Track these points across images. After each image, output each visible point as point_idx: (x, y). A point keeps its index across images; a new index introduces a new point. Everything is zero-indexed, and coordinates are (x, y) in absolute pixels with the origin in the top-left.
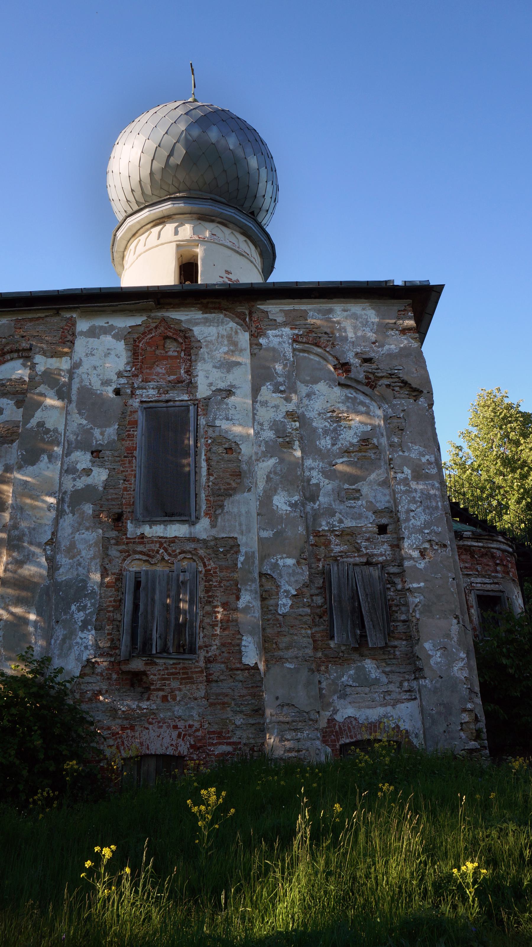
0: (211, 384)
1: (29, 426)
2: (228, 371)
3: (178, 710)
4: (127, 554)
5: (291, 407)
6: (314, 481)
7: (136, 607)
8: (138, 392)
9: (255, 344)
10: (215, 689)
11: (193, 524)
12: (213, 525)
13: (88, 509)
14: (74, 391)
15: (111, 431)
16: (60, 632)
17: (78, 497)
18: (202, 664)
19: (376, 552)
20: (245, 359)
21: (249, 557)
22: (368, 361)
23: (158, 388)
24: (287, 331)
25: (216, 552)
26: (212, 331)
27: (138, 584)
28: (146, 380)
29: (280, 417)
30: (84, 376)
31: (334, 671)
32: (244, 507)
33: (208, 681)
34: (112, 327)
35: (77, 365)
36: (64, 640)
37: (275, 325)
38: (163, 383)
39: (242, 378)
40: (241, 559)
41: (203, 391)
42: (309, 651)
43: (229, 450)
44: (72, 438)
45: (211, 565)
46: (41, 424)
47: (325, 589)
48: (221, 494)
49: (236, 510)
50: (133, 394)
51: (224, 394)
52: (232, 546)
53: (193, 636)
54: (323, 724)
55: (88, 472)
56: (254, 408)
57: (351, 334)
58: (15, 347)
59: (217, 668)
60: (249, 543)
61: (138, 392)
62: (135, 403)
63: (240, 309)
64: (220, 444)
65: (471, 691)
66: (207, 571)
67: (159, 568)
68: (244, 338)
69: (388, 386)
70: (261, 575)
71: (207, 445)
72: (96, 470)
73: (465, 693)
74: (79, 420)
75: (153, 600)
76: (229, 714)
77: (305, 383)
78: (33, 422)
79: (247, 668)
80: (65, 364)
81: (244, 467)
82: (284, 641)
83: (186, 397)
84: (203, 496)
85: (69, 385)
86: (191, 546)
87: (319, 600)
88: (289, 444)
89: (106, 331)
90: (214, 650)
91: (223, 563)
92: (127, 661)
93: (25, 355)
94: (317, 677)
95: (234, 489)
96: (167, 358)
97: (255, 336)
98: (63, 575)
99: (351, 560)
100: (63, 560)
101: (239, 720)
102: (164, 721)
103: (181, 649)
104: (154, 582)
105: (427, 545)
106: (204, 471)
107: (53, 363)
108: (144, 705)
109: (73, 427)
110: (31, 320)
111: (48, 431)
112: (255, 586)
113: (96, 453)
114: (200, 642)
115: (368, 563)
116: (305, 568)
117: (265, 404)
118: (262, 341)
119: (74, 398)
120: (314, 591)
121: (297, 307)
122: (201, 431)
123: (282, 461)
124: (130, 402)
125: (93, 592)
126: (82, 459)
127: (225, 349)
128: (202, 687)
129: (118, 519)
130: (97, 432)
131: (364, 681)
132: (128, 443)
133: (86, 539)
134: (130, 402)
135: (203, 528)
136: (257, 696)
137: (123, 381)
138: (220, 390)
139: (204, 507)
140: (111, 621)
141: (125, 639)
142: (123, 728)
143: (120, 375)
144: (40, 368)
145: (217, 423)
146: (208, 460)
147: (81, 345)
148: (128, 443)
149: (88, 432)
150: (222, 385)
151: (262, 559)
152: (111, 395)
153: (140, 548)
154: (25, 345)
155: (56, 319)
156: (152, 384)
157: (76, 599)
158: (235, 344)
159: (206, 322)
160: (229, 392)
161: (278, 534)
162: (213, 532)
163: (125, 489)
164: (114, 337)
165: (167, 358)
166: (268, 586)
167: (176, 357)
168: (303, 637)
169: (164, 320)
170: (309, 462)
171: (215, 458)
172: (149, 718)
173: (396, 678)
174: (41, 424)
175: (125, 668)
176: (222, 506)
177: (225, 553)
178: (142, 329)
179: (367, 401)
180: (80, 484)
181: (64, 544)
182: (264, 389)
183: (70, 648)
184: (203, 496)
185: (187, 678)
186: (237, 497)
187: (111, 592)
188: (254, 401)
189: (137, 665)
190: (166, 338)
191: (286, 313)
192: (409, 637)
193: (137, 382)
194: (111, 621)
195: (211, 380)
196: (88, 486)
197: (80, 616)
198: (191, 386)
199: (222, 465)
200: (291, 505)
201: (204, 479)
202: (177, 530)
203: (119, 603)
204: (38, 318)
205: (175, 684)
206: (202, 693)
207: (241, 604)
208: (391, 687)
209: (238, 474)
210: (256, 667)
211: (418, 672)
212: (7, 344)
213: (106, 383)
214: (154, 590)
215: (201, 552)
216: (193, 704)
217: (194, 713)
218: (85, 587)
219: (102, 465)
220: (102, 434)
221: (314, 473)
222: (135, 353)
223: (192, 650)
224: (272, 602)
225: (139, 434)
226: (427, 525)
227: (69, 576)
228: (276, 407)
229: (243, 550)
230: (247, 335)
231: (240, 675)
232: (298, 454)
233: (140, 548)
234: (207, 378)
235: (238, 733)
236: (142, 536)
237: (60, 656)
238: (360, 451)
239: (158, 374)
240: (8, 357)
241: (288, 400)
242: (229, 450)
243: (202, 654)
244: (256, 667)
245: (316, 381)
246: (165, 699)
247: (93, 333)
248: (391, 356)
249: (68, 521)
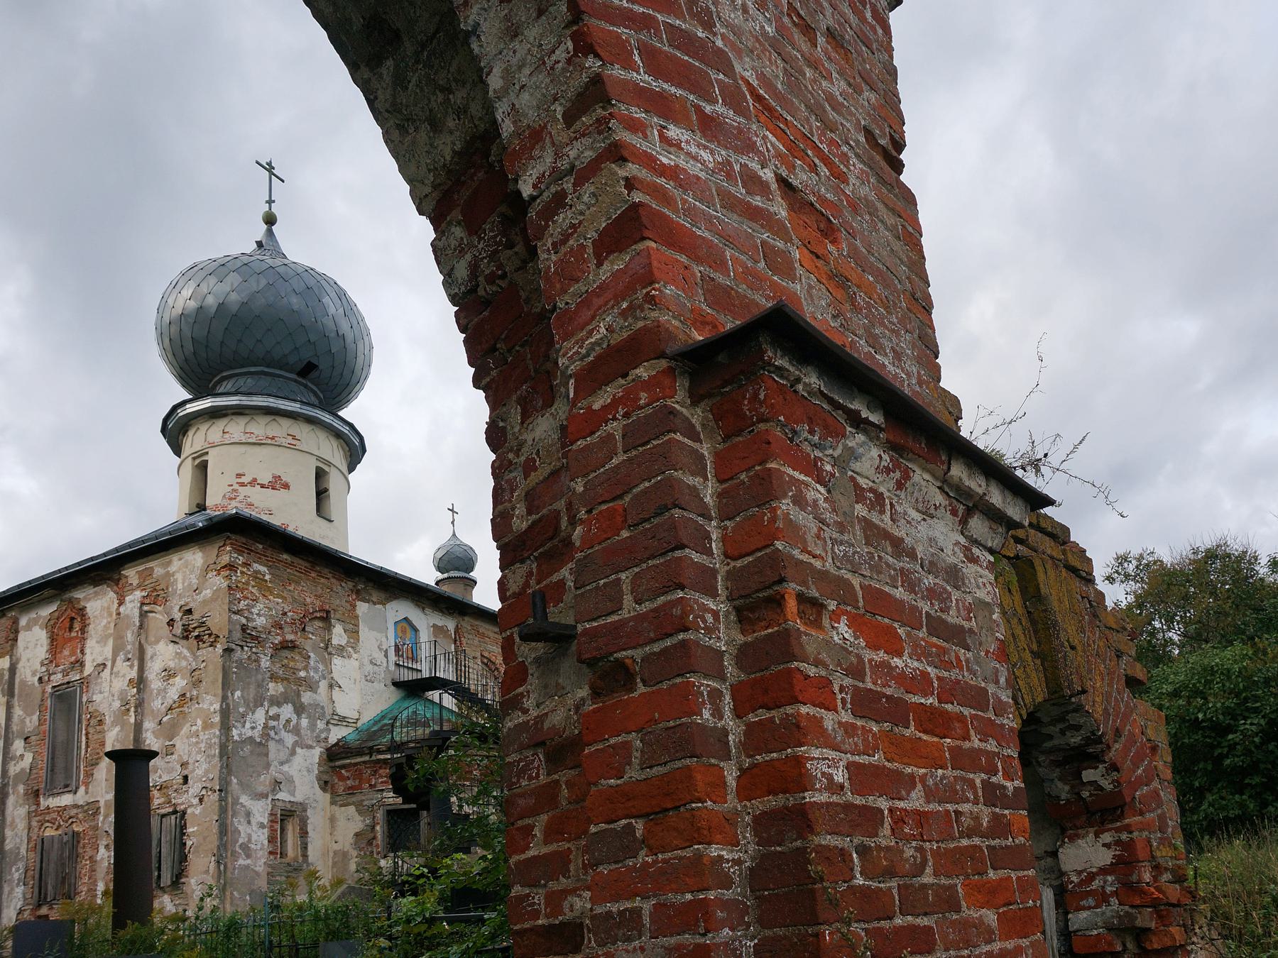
19: (180, 801)
22: (189, 612)
41: (88, 669)
57: (180, 586)
62: (49, 689)
69: (197, 637)
97: (120, 604)
105: (204, 792)
137: (44, 669)
138: (99, 665)
146: (87, 734)
150: (100, 661)
152: (37, 684)
171: (91, 730)
198: (80, 664)
226: (207, 772)
236: (48, 808)
245: (157, 642)
248: (205, 602)
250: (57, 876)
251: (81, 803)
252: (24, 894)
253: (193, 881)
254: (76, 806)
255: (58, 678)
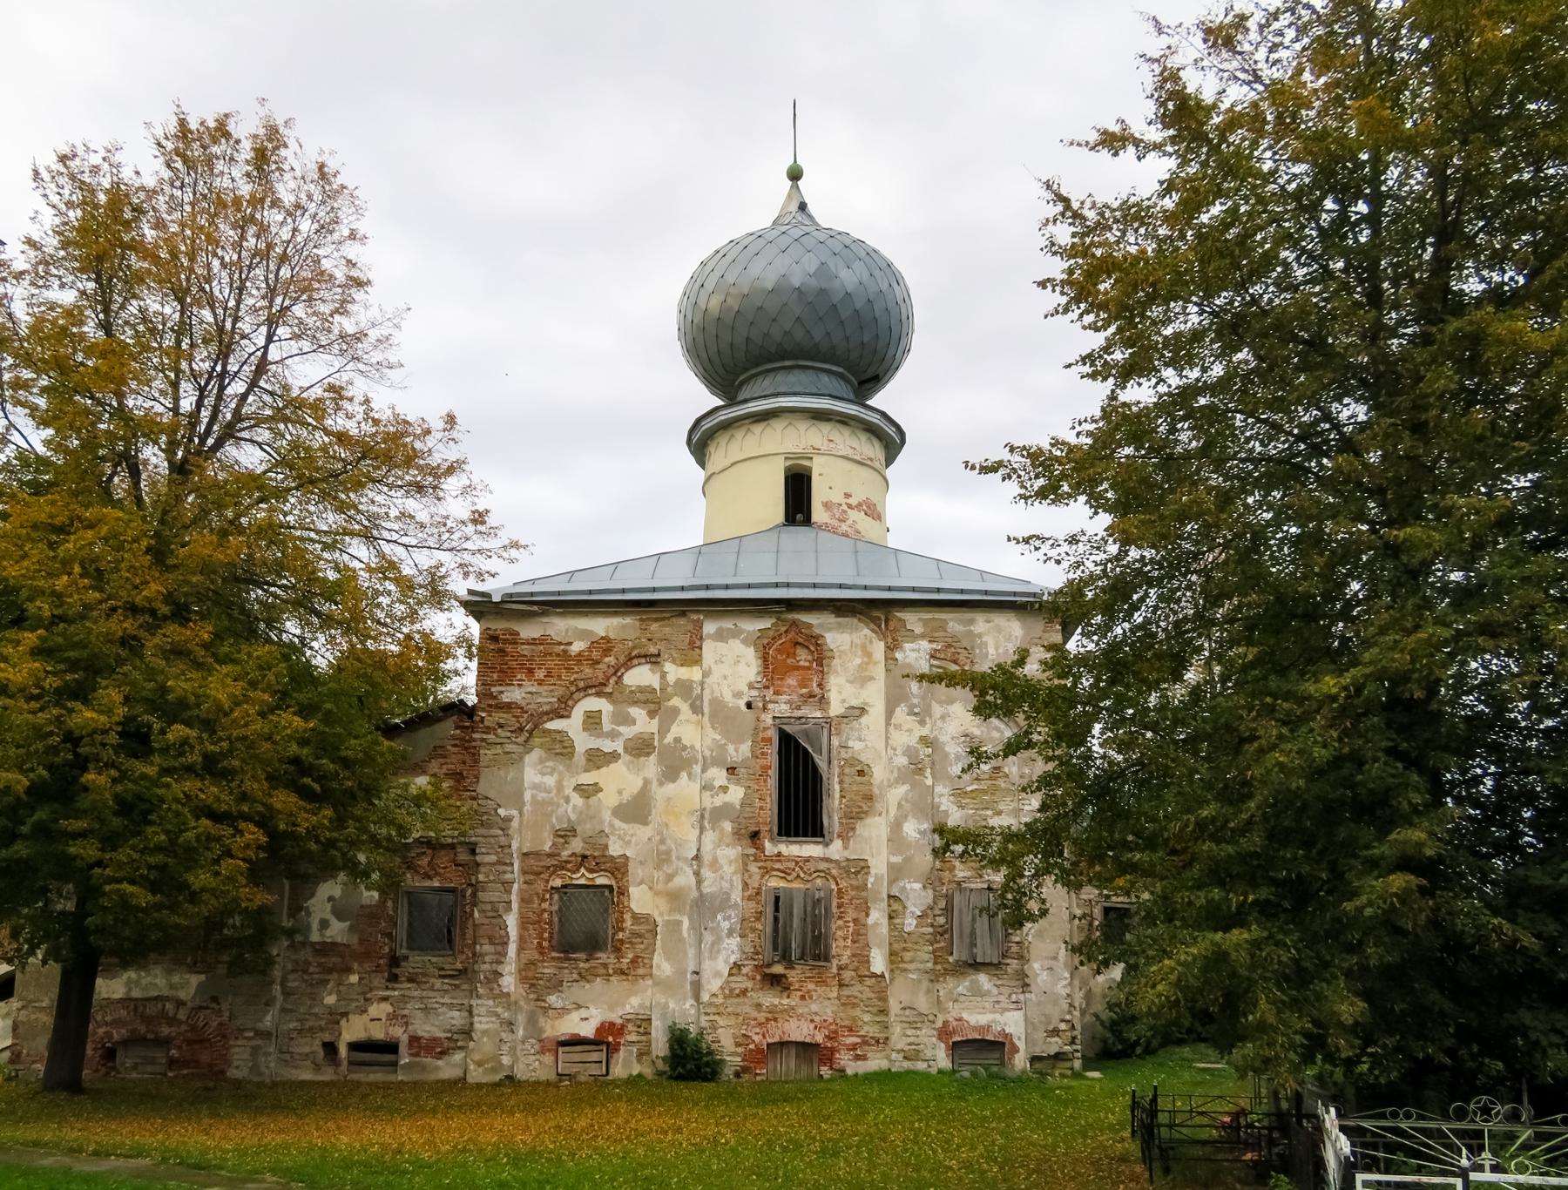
0: (844, 701)
1: (666, 741)
2: (862, 686)
3: (814, 1007)
4: (766, 871)
5: (925, 731)
6: (943, 808)
7: (776, 919)
8: (770, 706)
9: (890, 659)
10: (846, 992)
11: (827, 845)
12: (845, 848)
13: (728, 826)
14: (706, 703)
15: (745, 748)
16: (708, 938)
17: (718, 814)
18: (835, 970)
20: (879, 672)
21: (878, 878)
23: (789, 702)
24: (925, 645)
25: (848, 872)
26: (845, 641)
27: (777, 899)
28: (776, 693)
29: (913, 741)
30: (715, 687)
31: (951, 982)
32: (874, 830)
33: (841, 985)
34: (741, 631)
35: (706, 674)
36: (712, 945)
37: (914, 637)
38: (795, 697)
39: (874, 696)
40: (871, 880)
41: (836, 709)
42: (930, 965)
43: (861, 773)
44: (707, 753)
45: (843, 884)
46: (677, 740)
47: (948, 910)
48: (855, 816)
49: (866, 834)
50: (765, 708)
51: (857, 712)
52: (863, 867)
53: (828, 947)
54: (939, 1024)
55: (724, 789)
56: (887, 732)
58: (643, 652)
59: (847, 975)
60: (879, 866)
61: (770, 706)
63: (875, 614)
64: (852, 766)
65: (1071, 1005)
66: (840, 890)
67: (796, 885)
68: (879, 648)
70: (890, 897)
71: (841, 767)
72: (732, 788)
73: (1066, 1007)
74: (713, 735)
75: (791, 915)
76: (857, 1012)
77: (940, 703)
78: (669, 738)
79: (875, 976)
80: (695, 674)
81: (876, 791)
82: (908, 956)
83: (818, 714)
84: (836, 818)
85: (701, 697)
86: (824, 870)
87: (942, 920)
88: (920, 771)
89: (735, 634)
90: (845, 960)
91: (854, 883)
92: (769, 965)
93: (653, 659)
94: (937, 986)
95: (865, 813)
96: (798, 668)
97: (891, 648)
98: (707, 888)
99: (973, 886)
100: (706, 873)
101: (867, 1017)
102: (802, 1015)
103: (817, 958)
104: (791, 900)
106: (837, 795)
107: (684, 673)
108: (785, 1002)
109: (708, 741)
110: (656, 620)
111: (685, 748)
112: (884, 905)
113: (731, 770)
114: (834, 952)
115: (989, 889)
116: (930, 892)
117: (898, 727)
118: (898, 655)
119: (706, 710)
120: (937, 912)
121: (937, 616)
122: (834, 752)
123: (913, 787)
124: (763, 717)
125: (736, 904)
126: (719, 776)
127: (858, 661)
128: (835, 989)
129: (755, 836)
130: (731, 748)
131: (977, 992)
132: (762, 762)
133: (729, 855)
134: (763, 717)
135: (836, 850)
136: (884, 1000)
137: (755, 693)
139: (837, 828)
140: (753, 930)
141: (769, 946)
142: (768, 1020)
143: (751, 686)
144: (671, 679)
145: (850, 744)
146: (841, 782)
147: (710, 650)
148: (762, 762)
149: (722, 748)
150: (855, 703)
151: (891, 882)
152: (744, 708)
153: (777, 866)
154: (653, 650)
155: (682, 621)
156: (784, 698)
157: (722, 909)
158: (869, 655)
159: (839, 627)
160: (862, 710)
161: (907, 860)
162: (847, 854)
163: (761, 808)
164: (744, 642)
165: (798, 668)
166: (896, 906)
167: (809, 668)
168: (925, 953)
169: (794, 623)
170: (939, 789)
171: (847, 780)
172: (790, 1011)
173: (1006, 991)
174: (677, 740)
175: (767, 971)
176: (853, 829)
177: (856, 873)
178: (771, 633)
179: (1002, 726)
180: (719, 800)
181: (707, 858)
182: (898, 710)
183: (719, 951)
184: (836, 818)
185: (822, 982)
186: (869, 821)
187: (752, 904)
188: (888, 723)
189: (778, 969)
190: (797, 643)
191: (925, 622)
192: (1021, 957)
193: (769, 694)
194: (753, 930)
195: (844, 696)
196: (726, 804)
197: (726, 925)
198: (823, 701)
199: (855, 788)
200: (920, 832)
201: (837, 802)
202: (810, 849)
203: (759, 915)
204: (663, 619)
205: (811, 986)
206: (835, 994)
207: (870, 921)
208: (1001, 998)
209: (869, 798)
210: (882, 976)
211: (1025, 987)
212: (634, 648)
213: (738, 695)
214: (791, 907)
215: (834, 872)
216: (827, 1003)
217: (829, 1011)
218: (728, 899)
219: (738, 782)
220: (736, 750)
221: (944, 800)
222: (765, 659)
223: (827, 959)
224: (897, 921)
225: (772, 753)
227: (714, 889)
228: (910, 731)
229: (873, 871)
230: (882, 644)
231: (869, 982)
232: (929, 782)
233: (777, 866)
234: (840, 693)
235: (866, 1028)
236: (779, 855)
237: (710, 958)
238: (991, 778)
239: (789, 686)
240: (635, 662)
241: (922, 723)
242: (861, 773)
243: (835, 962)
244: (882, 976)
246: (803, 998)
247: (721, 636)
249: (709, 837)
250: (804, 935)
251: (836, 857)
252: (741, 948)
253: (1036, 966)
254: (827, 860)
255: (782, 708)
